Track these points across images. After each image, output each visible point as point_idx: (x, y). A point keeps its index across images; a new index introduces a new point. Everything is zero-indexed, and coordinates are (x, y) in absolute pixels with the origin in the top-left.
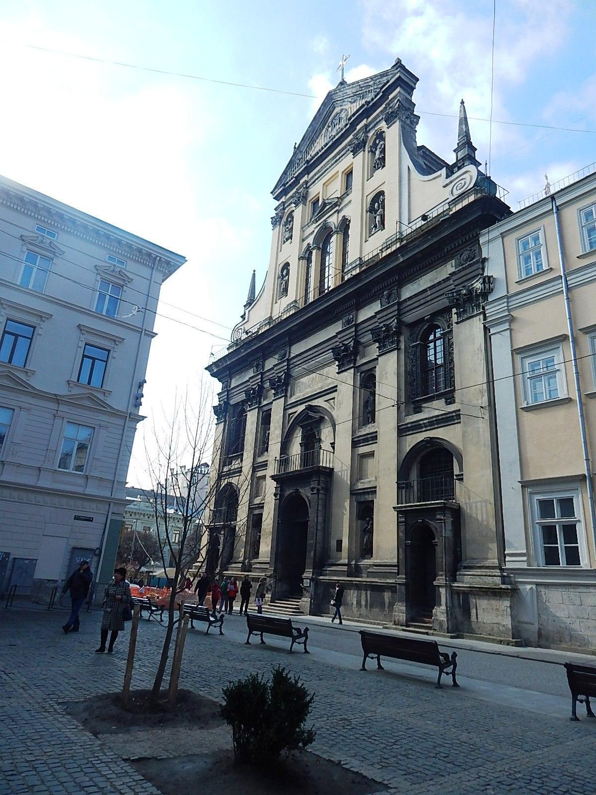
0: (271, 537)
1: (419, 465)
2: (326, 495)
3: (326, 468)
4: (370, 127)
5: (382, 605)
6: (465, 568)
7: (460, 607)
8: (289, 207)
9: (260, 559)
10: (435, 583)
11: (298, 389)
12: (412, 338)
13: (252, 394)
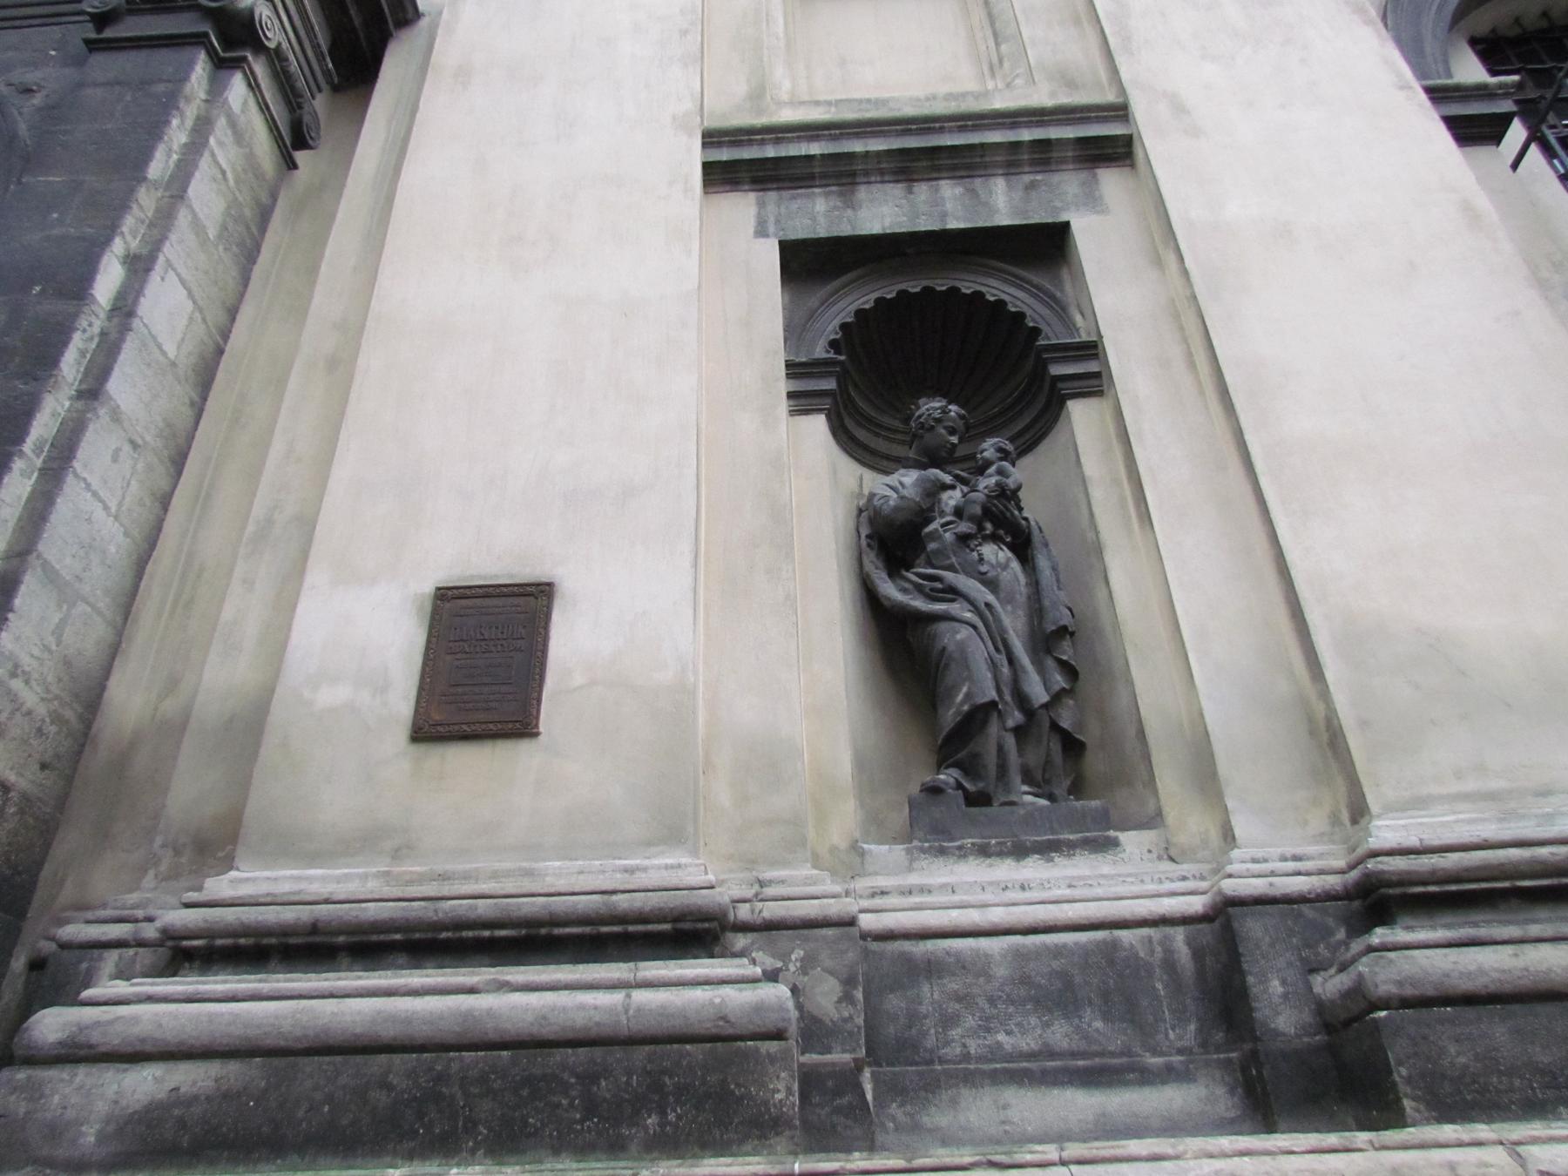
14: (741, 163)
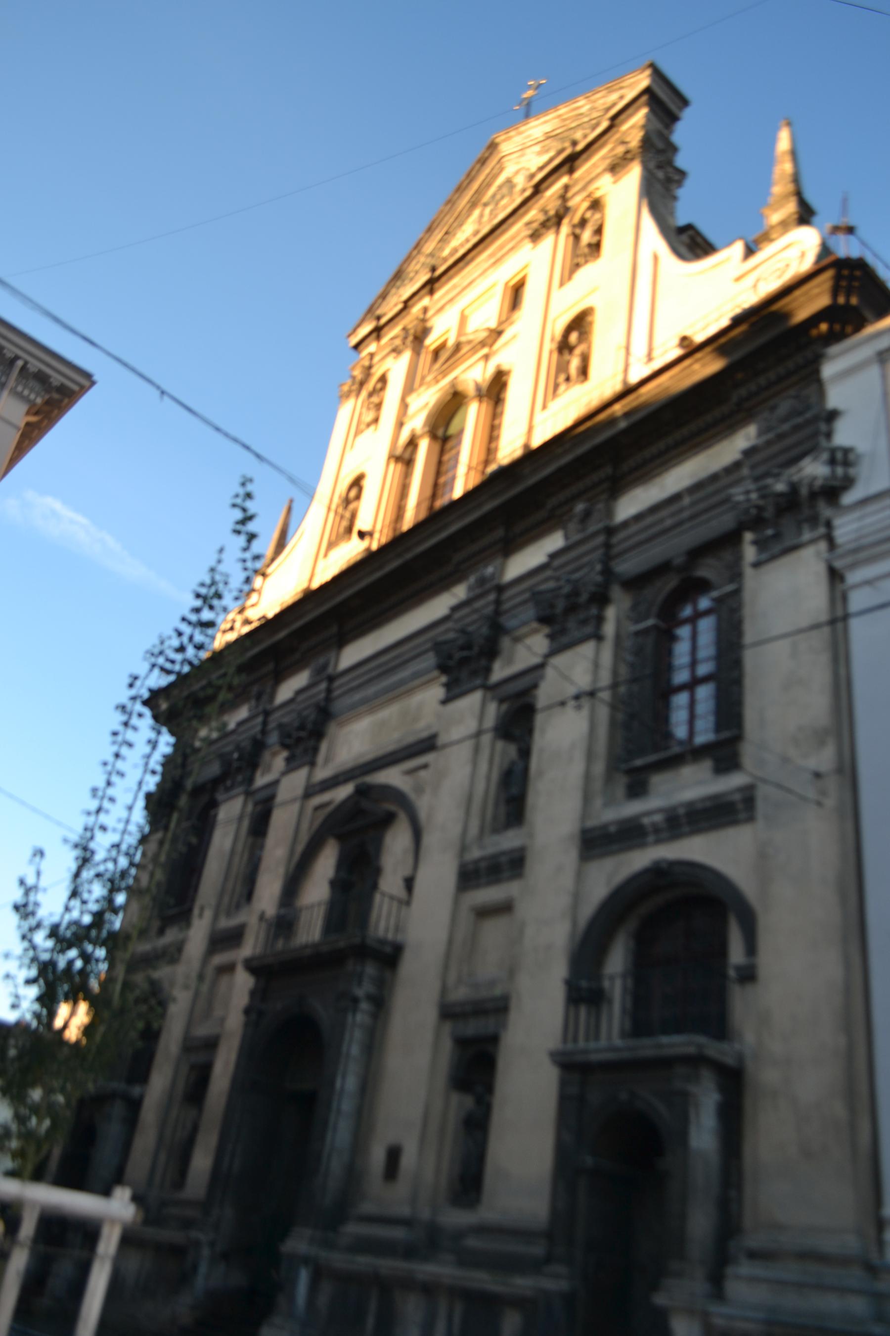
3: (383, 942)
6: (753, 1255)
10: (660, 1299)
12: (637, 613)
14: (448, 1012)
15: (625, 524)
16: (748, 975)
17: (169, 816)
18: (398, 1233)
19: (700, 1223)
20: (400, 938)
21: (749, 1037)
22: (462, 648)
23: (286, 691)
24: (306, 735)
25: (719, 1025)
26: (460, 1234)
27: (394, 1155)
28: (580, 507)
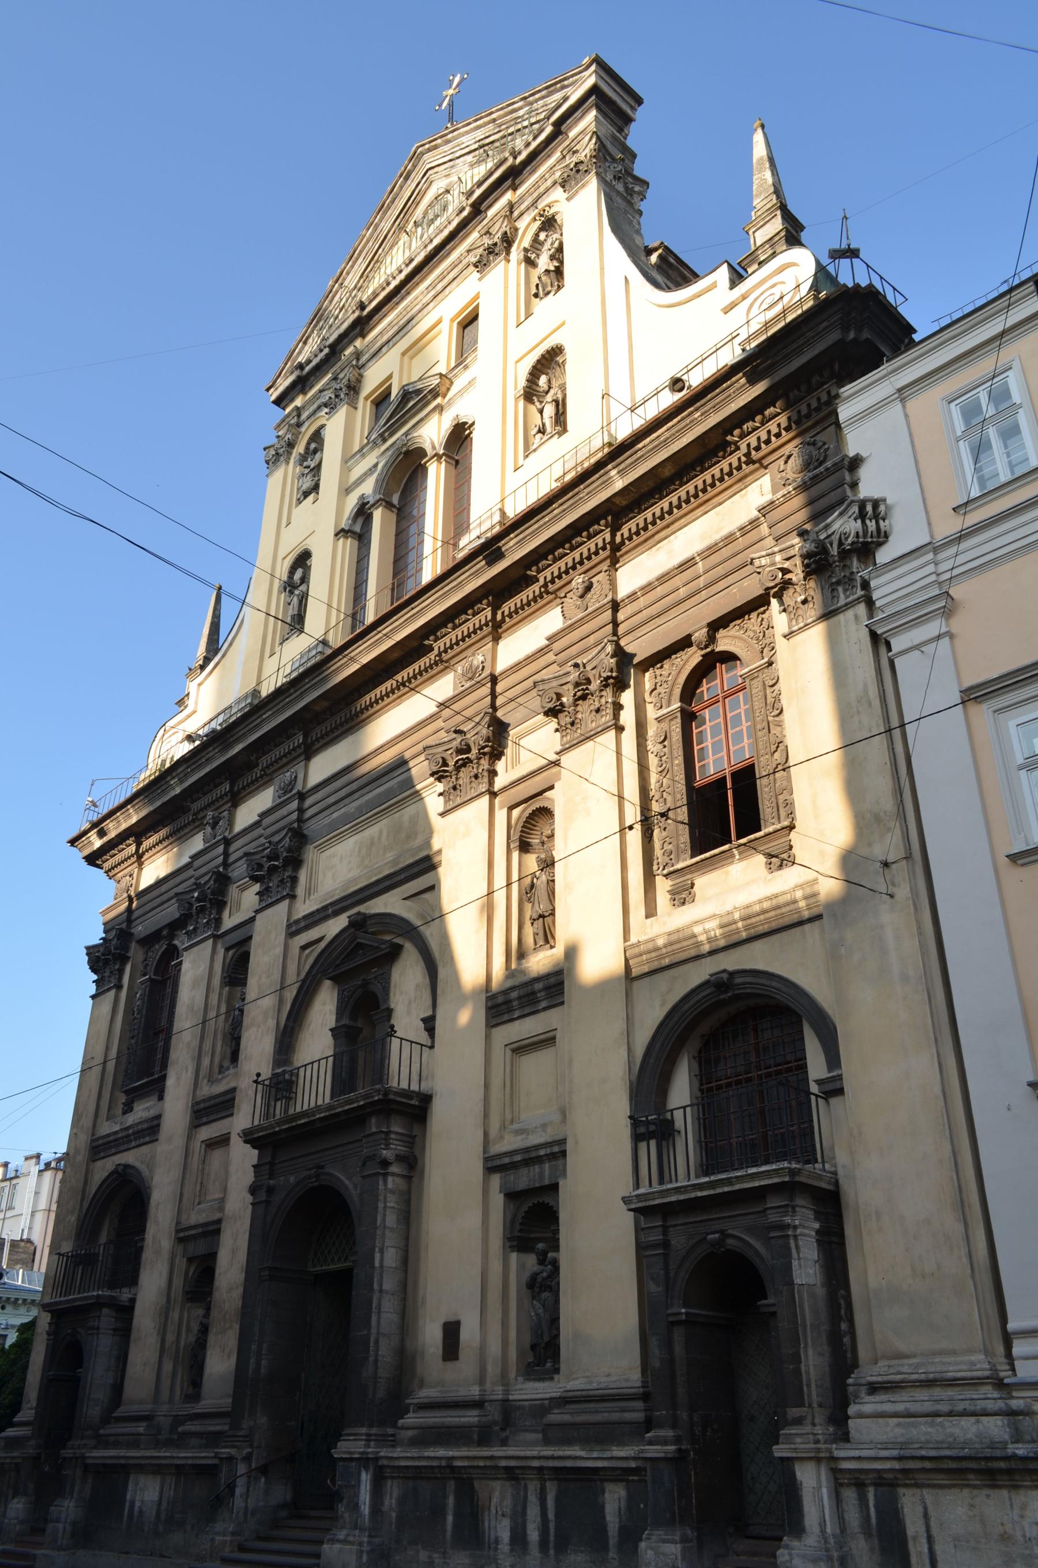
0: (237, 1327)
1: (696, 1065)
2: (408, 1178)
3: (407, 1094)
4: (523, 207)
5: (597, 1540)
6: (874, 1389)
7: (867, 1533)
8: (313, 418)
9: (203, 1402)
10: (780, 1451)
11: (330, 874)
13: (198, 900)
14: (495, 1165)
15: (633, 597)
16: (833, 1089)
17: (121, 972)
18: (471, 1417)
19: (814, 1362)
20: (425, 1087)
21: (842, 1158)
22: (459, 751)
23: (247, 813)
24: (279, 865)
25: (802, 1142)
26: (542, 1408)
27: (451, 1330)
28: (578, 581)
